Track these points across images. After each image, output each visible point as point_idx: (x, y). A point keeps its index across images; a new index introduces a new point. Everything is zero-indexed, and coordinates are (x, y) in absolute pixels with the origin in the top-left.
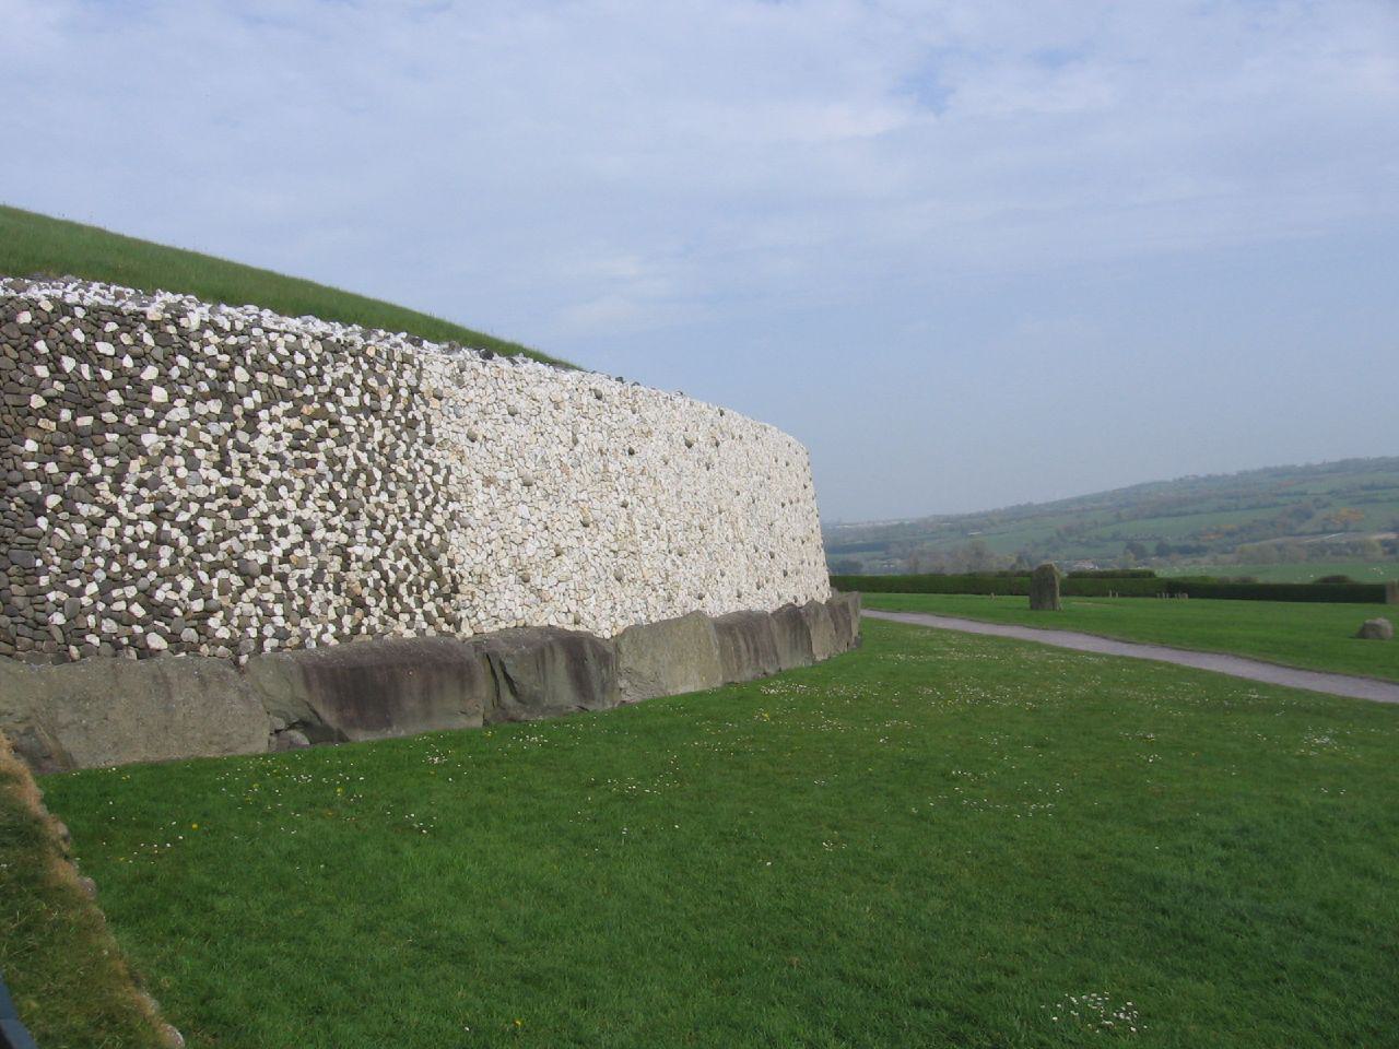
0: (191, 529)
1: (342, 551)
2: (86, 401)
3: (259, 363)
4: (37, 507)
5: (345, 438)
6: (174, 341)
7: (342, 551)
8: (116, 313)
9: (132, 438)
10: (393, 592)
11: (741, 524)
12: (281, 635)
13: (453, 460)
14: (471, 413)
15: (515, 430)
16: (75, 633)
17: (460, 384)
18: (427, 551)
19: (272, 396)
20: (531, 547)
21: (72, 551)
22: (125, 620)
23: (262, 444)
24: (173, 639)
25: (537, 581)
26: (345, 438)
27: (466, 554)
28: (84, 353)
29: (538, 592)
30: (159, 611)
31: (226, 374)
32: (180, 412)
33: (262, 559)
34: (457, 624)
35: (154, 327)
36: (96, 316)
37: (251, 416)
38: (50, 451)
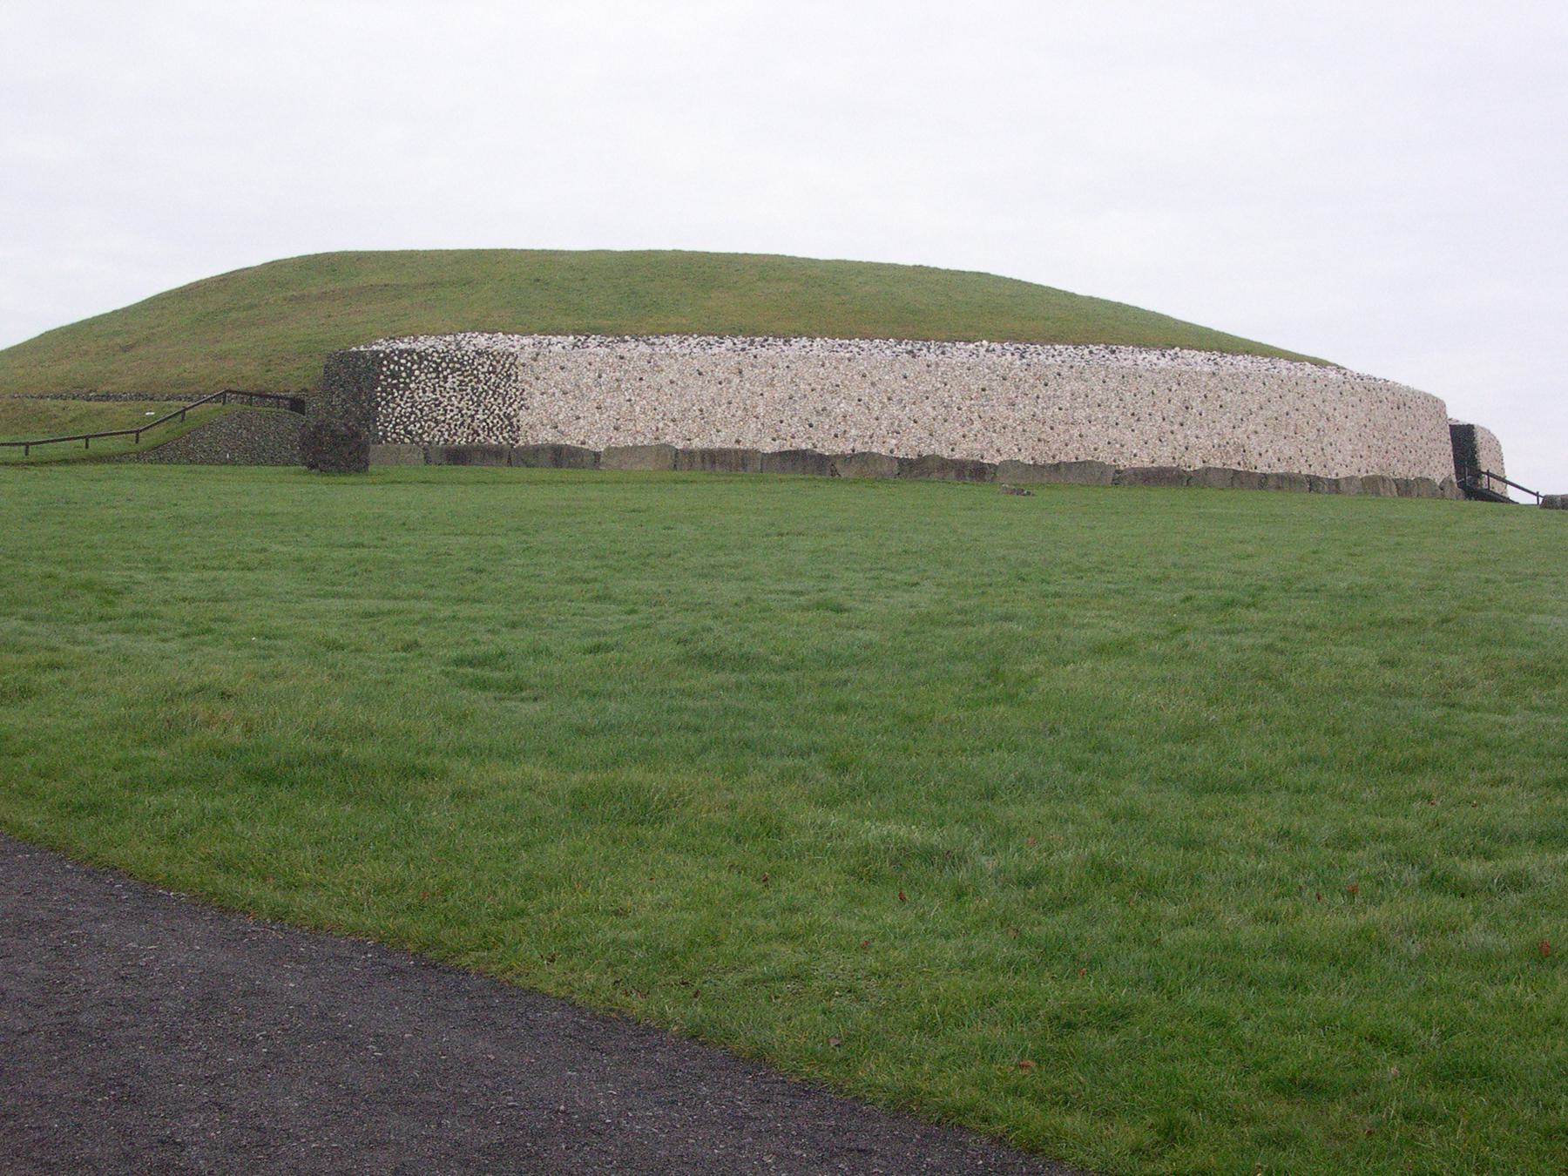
0: (421, 410)
2: (394, 375)
3: (451, 361)
4: (378, 404)
5: (479, 382)
6: (422, 357)
8: (406, 351)
11: (761, 410)
14: (537, 370)
15: (563, 374)
16: (385, 437)
18: (508, 416)
19: (453, 371)
21: (387, 416)
24: (412, 441)
25: (561, 427)
26: (479, 382)
27: (525, 418)
28: (396, 363)
30: (410, 433)
31: (439, 365)
32: (423, 377)
36: (401, 352)
37: (446, 378)
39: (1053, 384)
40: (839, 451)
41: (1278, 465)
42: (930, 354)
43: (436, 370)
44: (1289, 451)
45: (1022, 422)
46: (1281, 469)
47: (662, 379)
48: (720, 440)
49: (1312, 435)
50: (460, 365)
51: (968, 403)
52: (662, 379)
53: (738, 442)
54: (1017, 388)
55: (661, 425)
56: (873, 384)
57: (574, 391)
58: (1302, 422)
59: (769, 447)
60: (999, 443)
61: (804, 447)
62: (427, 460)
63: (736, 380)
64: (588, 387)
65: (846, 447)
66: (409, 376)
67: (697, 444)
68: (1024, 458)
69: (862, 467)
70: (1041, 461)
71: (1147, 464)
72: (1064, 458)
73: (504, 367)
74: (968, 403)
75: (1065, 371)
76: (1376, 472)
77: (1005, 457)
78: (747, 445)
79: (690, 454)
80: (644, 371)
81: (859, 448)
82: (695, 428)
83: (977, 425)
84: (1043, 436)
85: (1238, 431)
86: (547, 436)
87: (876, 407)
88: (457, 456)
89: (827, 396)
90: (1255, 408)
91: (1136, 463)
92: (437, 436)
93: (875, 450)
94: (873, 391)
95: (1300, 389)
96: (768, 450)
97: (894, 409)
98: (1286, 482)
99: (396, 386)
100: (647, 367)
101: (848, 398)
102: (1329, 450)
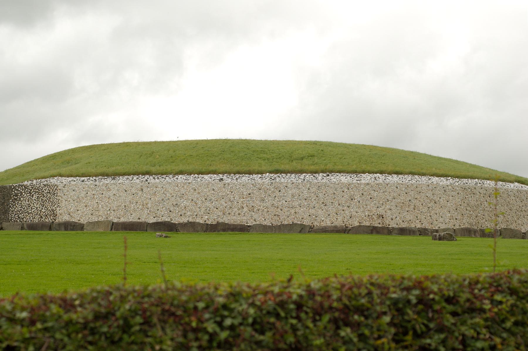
0: (24, 209)
1: (41, 211)
4: (10, 207)
5: (44, 196)
7: (41, 211)
9: (20, 198)
10: (46, 216)
11: (149, 205)
12: (31, 221)
13: (60, 198)
16: (11, 220)
17: (64, 187)
20: (72, 210)
21: (12, 211)
22: (16, 218)
23: (33, 198)
24: (20, 221)
25: (72, 214)
27: (58, 212)
28: (17, 190)
29: (71, 216)
30: (19, 218)
31: (31, 190)
32: (25, 195)
33: (30, 211)
34: (55, 220)
35: (25, 186)
37: (33, 195)
38: (12, 201)
39: (283, 191)
40: (182, 221)
41: (402, 224)
42: (227, 179)
43: (30, 193)
44: (408, 218)
45: (267, 208)
46: (404, 225)
47: (110, 194)
48: (132, 218)
49: (425, 210)
50: (38, 190)
51: (242, 200)
52: (110, 194)
53: (139, 219)
54: (266, 192)
55: (109, 212)
56: (199, 193)
57: (79, 200)
58: (418, 204)
59: (152, 220)
60: (255, 216)
61: (167, 220)
62: (22, 228)
63: (140, 193)
64: (83, 198)
65: (184, 220)
66: (21, 195)
67: (122, 220)
68: (267, 223)
69: (191, 227)
70: (275, 224)
71: (329, 224)
72: (286, 223)
73: (53, 190)
74: (242, 200)
75: (289, 185)
76: (467, 226)
77: (258, 223)
78: (143, 220)
79: (117, 224)
80: (103, 190)
81: (191, 220)
82: (122, 213)
83: (246, 209)
84: (277, 213)
85: (380, 209)
86: (66, 218)
87: (199, 202)
88: (32, 227)
89: (179, 199)
90: (390, 198)
91: (323, 224)
92: (29, 219)
93: (197, 221)
94: (198, 196)
95: (418, 189)
96: (151, 221)
97: (208, 204)
98: (403, 231)
99: (16, 199)
100: (105, 189)
101: (187, 199)
102: (434, 217)
